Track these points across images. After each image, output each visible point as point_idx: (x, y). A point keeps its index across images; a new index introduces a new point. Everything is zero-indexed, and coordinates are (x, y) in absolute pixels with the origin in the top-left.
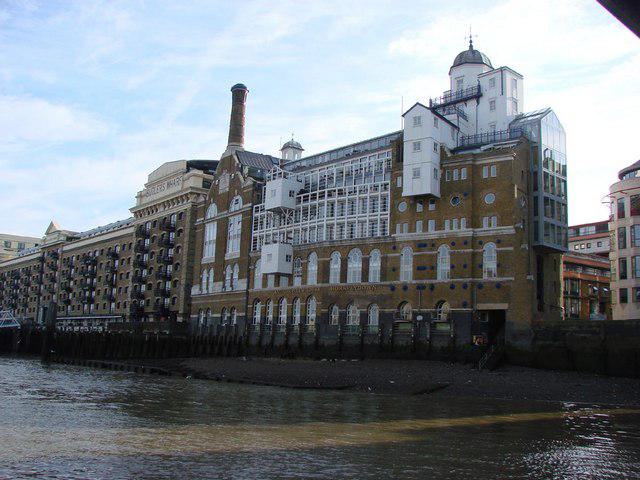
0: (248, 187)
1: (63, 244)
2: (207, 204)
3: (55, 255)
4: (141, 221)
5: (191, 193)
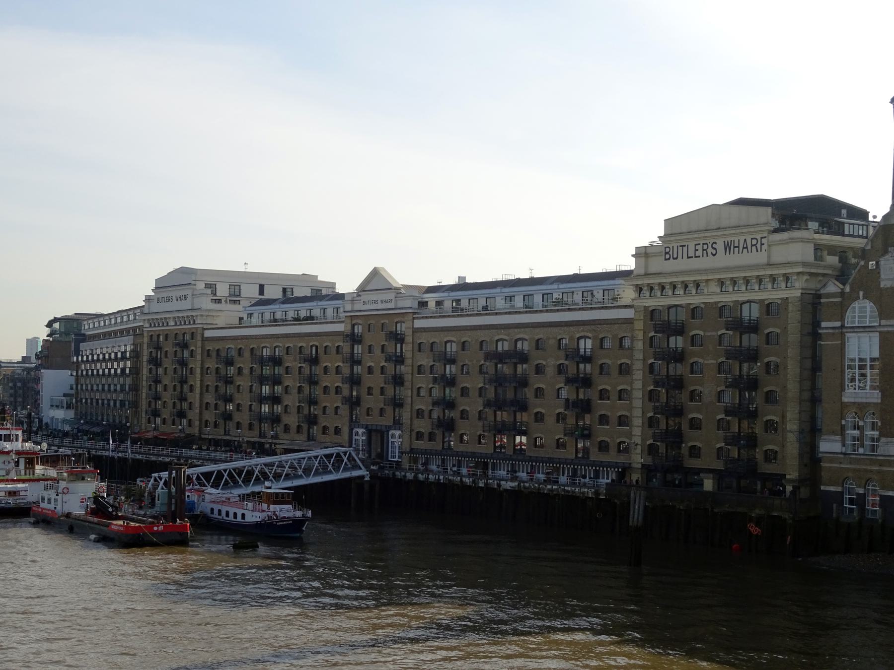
1: (414, 316)
2: (844, 302)
4: (657, 302)
5: (799, 273)
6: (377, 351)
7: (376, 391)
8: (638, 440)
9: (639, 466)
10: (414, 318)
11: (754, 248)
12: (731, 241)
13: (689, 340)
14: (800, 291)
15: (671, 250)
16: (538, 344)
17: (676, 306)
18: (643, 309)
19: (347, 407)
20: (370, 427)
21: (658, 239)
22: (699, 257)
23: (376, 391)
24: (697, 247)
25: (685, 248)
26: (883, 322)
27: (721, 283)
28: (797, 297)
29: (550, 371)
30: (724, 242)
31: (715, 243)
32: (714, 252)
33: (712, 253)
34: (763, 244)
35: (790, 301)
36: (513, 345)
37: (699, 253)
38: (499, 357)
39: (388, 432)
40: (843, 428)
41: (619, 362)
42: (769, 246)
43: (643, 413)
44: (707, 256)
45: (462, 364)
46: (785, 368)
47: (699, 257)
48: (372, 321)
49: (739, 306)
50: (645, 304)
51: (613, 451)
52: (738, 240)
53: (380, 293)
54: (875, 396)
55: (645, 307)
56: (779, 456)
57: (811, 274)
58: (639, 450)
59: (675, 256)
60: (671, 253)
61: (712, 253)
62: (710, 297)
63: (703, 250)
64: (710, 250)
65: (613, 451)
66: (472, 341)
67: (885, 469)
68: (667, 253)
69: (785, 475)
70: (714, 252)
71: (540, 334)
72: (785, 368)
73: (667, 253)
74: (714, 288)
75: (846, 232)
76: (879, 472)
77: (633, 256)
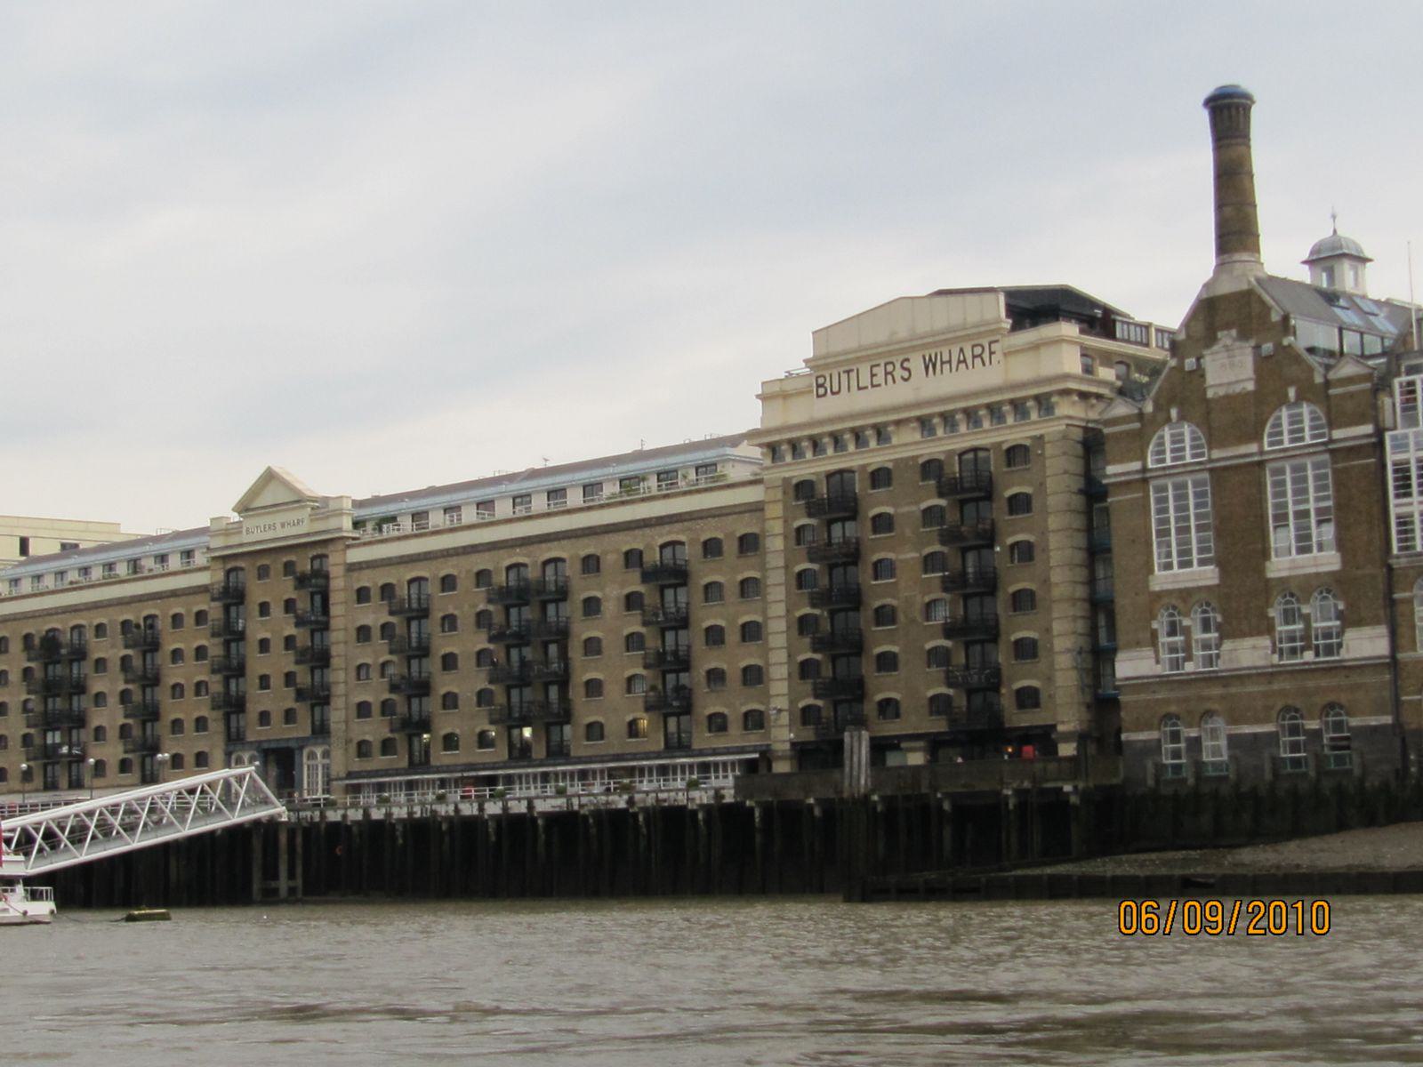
0: (1350, 380)
2: (1145, 428)
3: (315, 584)
6: (277, 610)
7: (277, 681)
8: (782, 703)
9: (787, 746)
10: (348, 547)
11: (978, 361)
13: (869, 524)
15: (828, 379)
16: (591, 564)
18: (780, 483)
19: (219, 714)
20: (266, 746)
21: (803, 365)
22: (879, 385)
23: (277, 681)
24: (875, 370)
25: (853, 375)
26: (1216, 454)
27: (924, 423)
28: (1060, 432)
29: (611, 607)
31: (907, 360)
32: (906, 374)
34: (994, 353)
35: (1046, 439)
36: (539, 568)
37: (879, 379)
38: (517, 594)
39: (301, 748)
40: (1154, 634)
41: (740, 577)
42: (1005, 355)
43: (789, 656)
44: (894, 382)
45: (441, 614)
46: (1043, 550)
48: (263, 558)
49: (957, 458)
50: (787, 475)
51: (735, 729)
53: (278, 511)
54: (1208, 575)
56: (1043, 697)
58: (785, 718)
59: (835, 389)
60: (828, 385)
64: (899, 373)
65: (735, 729)
66: (460, 572)
67: (1233, 690)
68: (822, 386)
69: (1053, 727)
71: (588, 547)
72: (1046, 550)
73: (822, 386)
74: (911, 435)
75: (1118, 335)
76: (1223, 697)
77: (758, 396)
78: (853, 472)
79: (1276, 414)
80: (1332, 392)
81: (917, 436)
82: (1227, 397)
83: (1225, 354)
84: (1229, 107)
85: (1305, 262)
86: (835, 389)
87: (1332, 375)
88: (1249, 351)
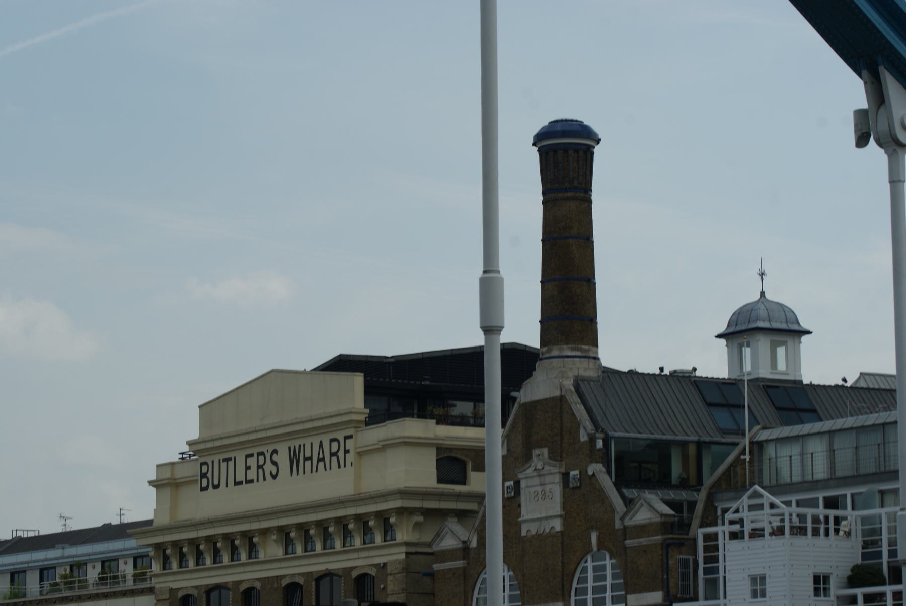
0: (642, 529)
5: (400, 511)
11: (334, 459)
12: (300, 446)
14: (403, 549)
17: (218, 587)
18: (167, 596)
22: (251, 481)
25: (231, 464)
28: (400, 562)
30: (290, 448)
33: (271, 473)
37: (252, 474)
42: (360, 454)
44: (264, 479)
47: (251, 481)
49: (313, 583)
50: (174, 586)
52: (311, 444)
55: (172, 591)
57: (428, 513)
59: (216, 482)
60: (209, 475)
61: (271, 473)
62: (268, 566)
63: (259, 467)
64: (269, 468)
70: (274, 473)
74: (272, 549)
77: (151, 483)
78: (228, 589)
79: (582, 565)
80: (628, 542)
81: (277, 551)
82: (539, 537)
83: (537, 481)
84: (577, 148)
85: (719, 336)
86: (216, 482)
87: (628, 522)
88: (557, 478)
